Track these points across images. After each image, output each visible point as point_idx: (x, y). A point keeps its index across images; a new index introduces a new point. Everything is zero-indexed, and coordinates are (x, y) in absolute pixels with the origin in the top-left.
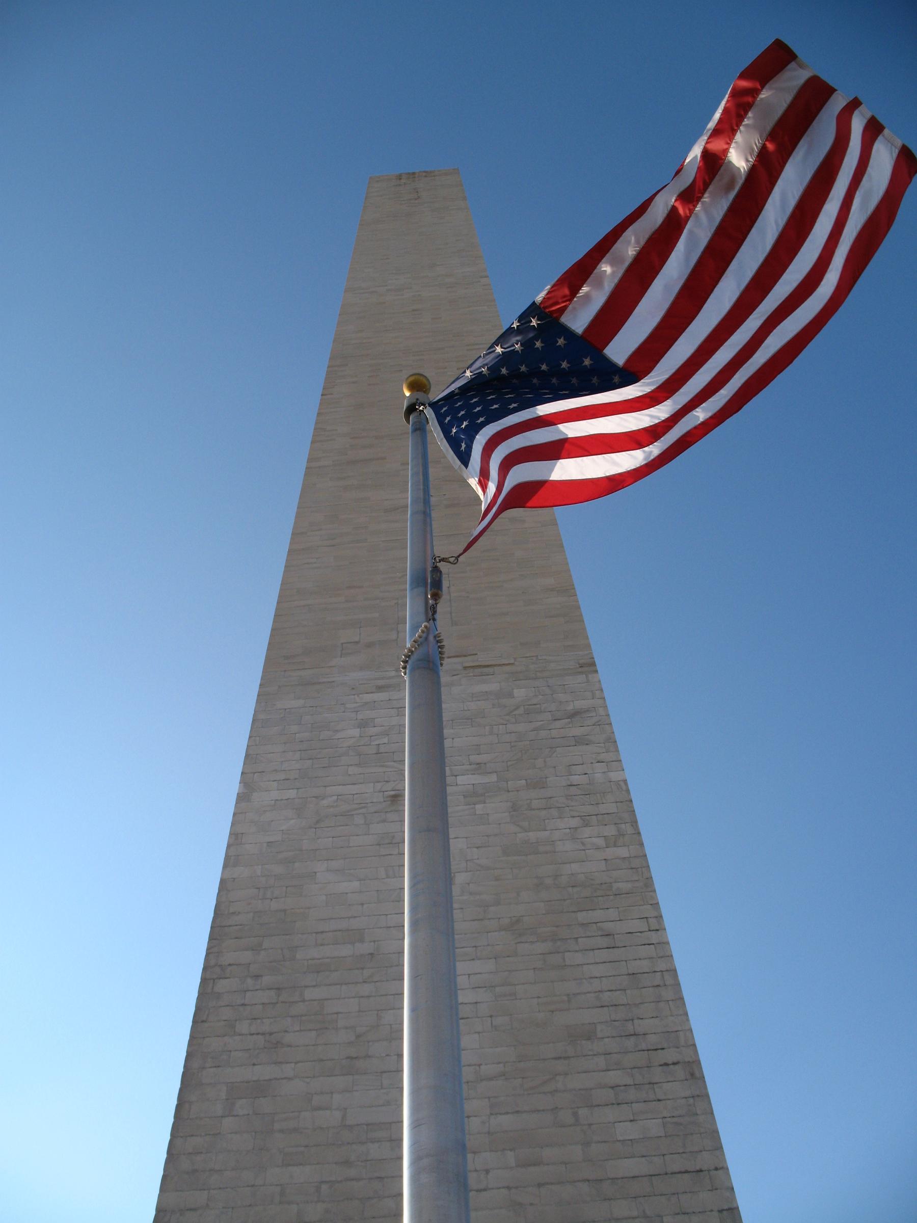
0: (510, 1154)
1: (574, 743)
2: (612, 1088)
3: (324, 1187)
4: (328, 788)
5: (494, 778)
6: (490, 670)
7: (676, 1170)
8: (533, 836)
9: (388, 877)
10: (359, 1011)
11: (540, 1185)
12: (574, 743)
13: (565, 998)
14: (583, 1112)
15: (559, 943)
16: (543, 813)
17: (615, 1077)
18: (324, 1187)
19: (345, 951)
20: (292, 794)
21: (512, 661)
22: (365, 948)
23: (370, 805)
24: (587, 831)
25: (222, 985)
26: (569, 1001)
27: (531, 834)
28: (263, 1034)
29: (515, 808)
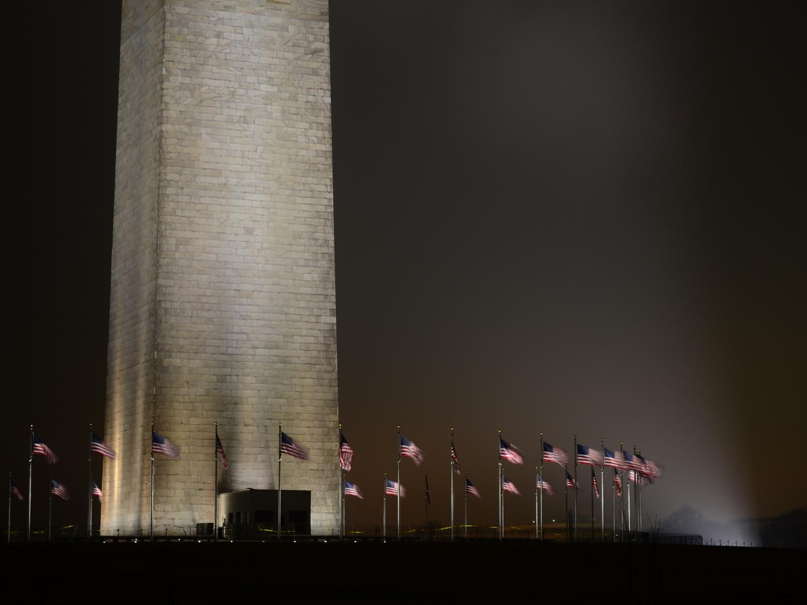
0: (270, 280)
1: (311, 73)
2: (305, 259)
3: (212, 284)
4: (204, 80)
5: (275, 89)
6: (278, 6)
7: (320, 294)
8: (290, 130)
9: (230, 143)
10: (221, 212)
11: (278, 293)
12: (311, 73)
13: (293, 218)
14: (295, 268)
15: (294, 191)
16: (295, 117)
17: (306, 255)
18: (212, 284)
19: (215, 180)
20: (187, 80)
21: (289, 2)
22: (223, 180)
23: (223, 95)
24: (311, 132)
25: (169, 191)
26: (295, 220)
27: (289, 129)
28: (186, 217)
29: (283, 111)
